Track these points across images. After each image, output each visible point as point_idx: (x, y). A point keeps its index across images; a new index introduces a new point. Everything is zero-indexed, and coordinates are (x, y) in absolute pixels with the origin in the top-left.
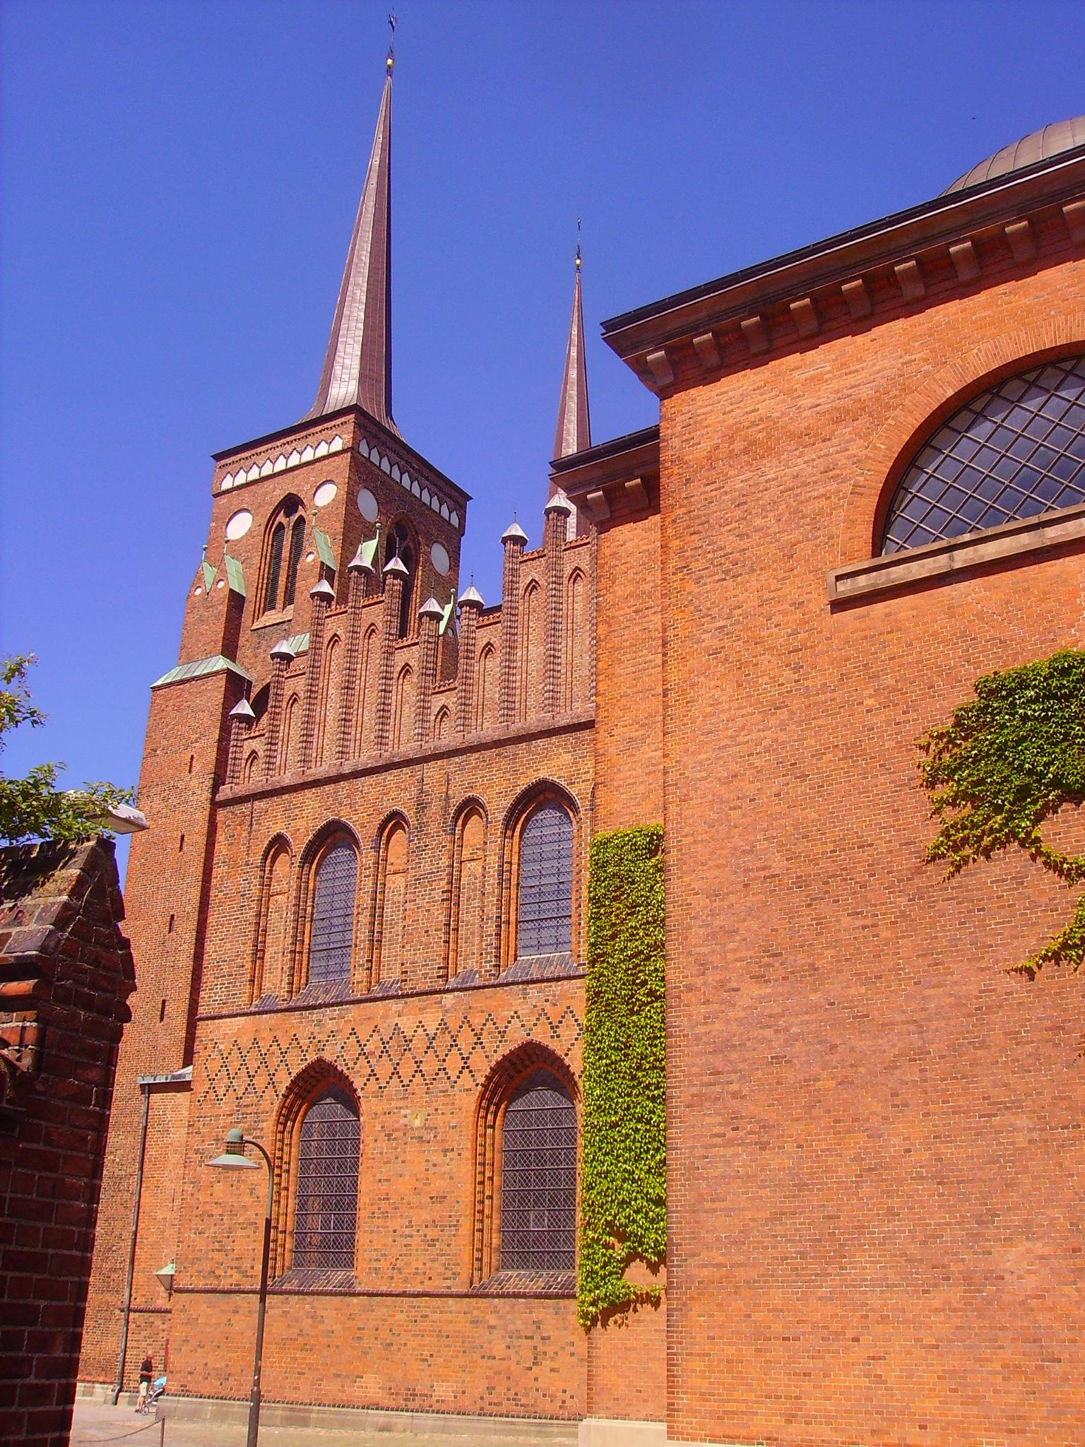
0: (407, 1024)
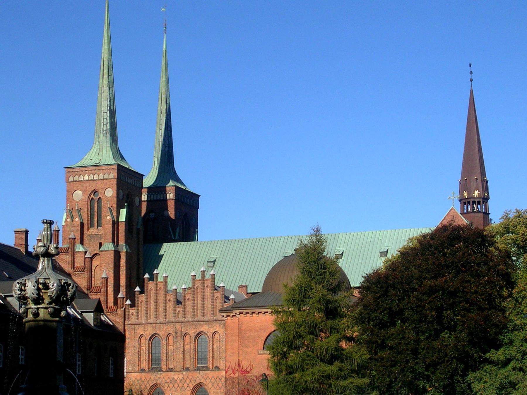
0: (176, 377)
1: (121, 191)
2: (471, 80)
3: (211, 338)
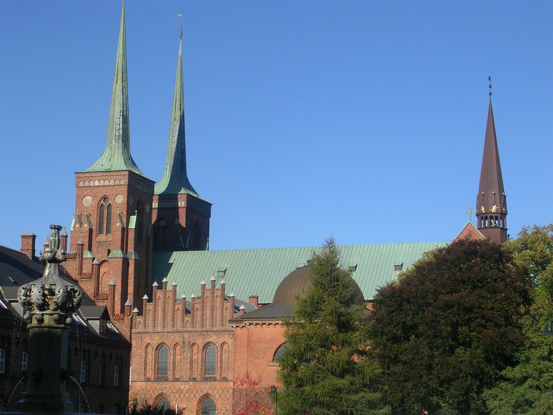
0: (182, 387)
1: (131, 197)
2: (490, 94)
3: (219, 349)
